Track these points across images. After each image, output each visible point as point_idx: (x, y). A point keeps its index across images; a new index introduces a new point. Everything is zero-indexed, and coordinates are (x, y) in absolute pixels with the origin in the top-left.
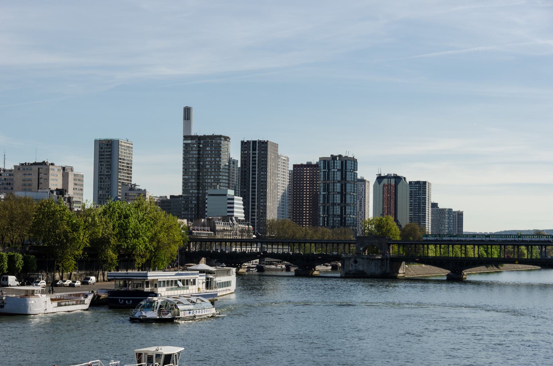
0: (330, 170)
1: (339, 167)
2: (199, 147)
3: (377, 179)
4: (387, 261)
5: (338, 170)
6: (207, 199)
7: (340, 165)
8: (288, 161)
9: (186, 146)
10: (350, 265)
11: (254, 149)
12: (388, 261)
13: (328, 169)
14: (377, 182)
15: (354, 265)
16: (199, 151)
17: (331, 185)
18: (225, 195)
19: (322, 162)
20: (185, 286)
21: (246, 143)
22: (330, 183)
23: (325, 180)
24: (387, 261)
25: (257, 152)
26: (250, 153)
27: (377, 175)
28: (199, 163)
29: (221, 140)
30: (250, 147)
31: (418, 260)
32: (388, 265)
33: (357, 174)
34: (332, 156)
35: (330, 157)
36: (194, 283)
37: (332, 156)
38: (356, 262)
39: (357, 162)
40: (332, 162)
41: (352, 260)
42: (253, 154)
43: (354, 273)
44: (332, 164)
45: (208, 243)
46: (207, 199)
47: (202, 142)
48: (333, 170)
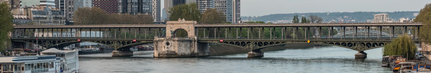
4: (194, 43)
10: (163, 47)
12: (196, 43)
15: (166, 46)
20: (37, 69)
24: (194, 43)
31: (223, 41)
32: (196, 46)
36: (52, 66)
38: (168, 44)
41: (165, 42)
43: (166, 54)
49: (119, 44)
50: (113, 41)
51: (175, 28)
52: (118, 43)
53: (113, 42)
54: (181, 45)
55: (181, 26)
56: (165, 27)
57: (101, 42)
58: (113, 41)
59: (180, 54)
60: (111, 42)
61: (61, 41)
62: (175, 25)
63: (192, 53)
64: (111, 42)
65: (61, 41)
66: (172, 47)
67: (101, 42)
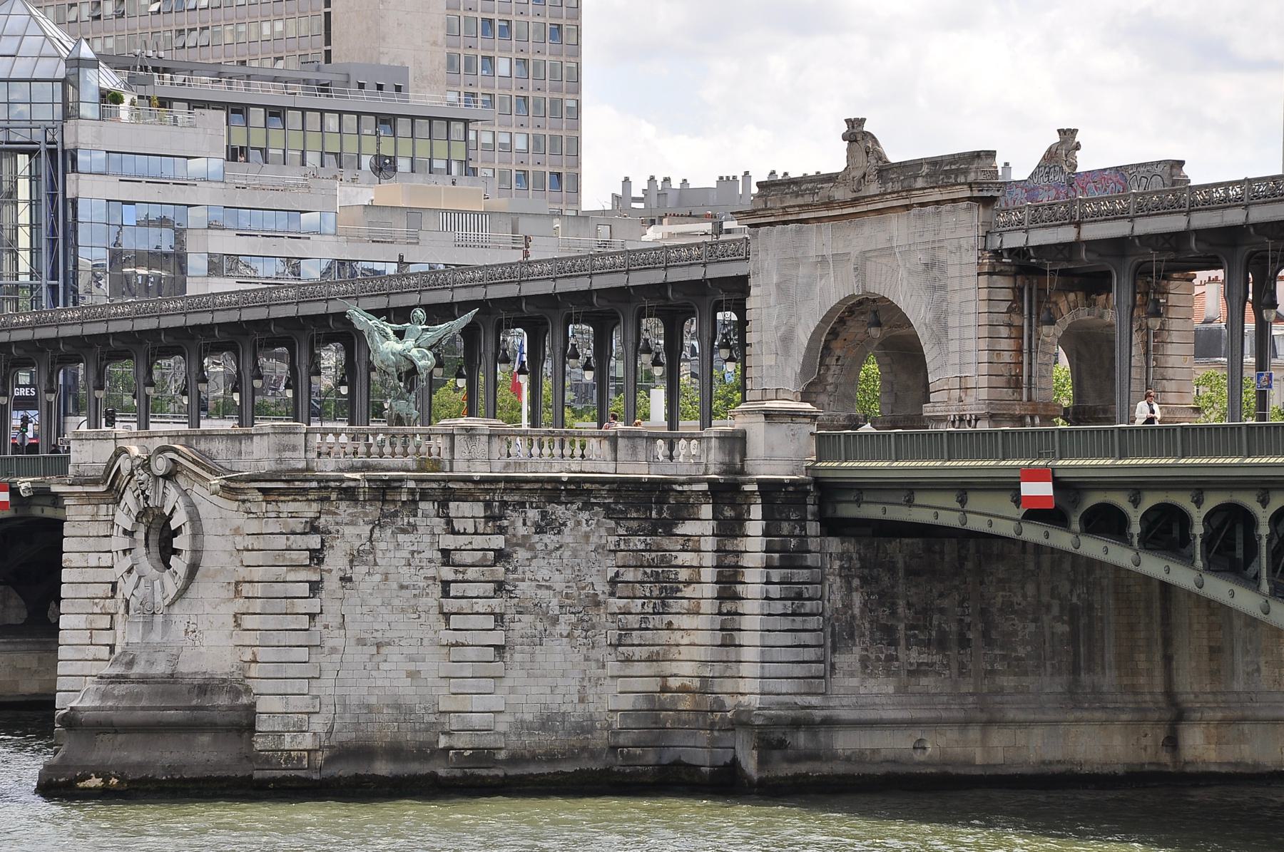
4: (730, 528)
24: (730, 528)
54: (336, 561)
55: (864, 256)
59: (318, 724)
63: (686, 703)
66: (207, 591)
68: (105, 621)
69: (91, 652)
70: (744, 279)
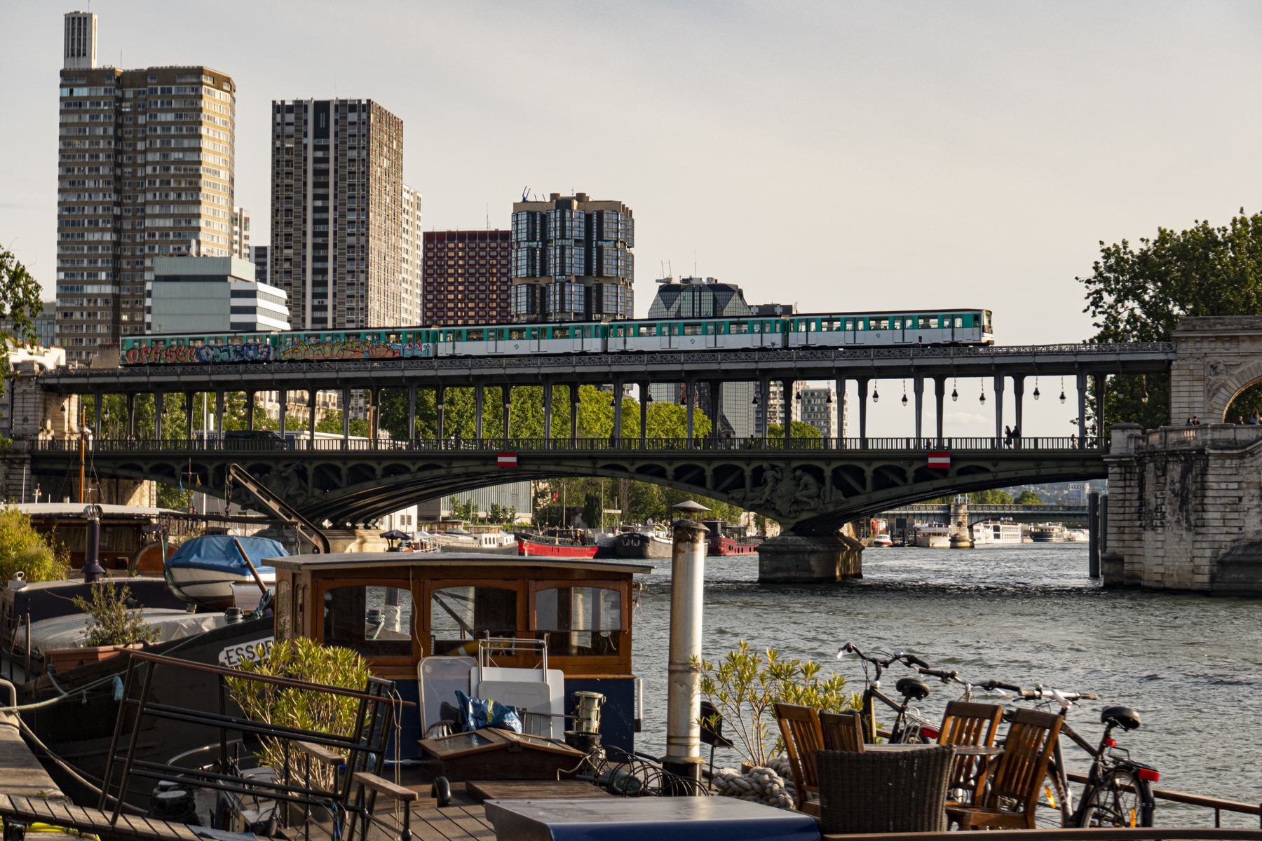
0: (550, 241)
1: (578, 231)
2: (119, 113)
3: (660, 292)
5: (576, 241)
6: (149, 294)
7: (583, 225)
8: (419, 208)
9: (69, 106)
11: (321, 132)
13: (541, 240)
14: (661, 302)
16: (118, 126)
17: (553, 290)
18: (223, 278)
19: (525, 216)
21: (290, 109)
22: (547, 285)
23: (534, 276)
25: (332, 142)
26: (306, 146)
27: (657, 281)
28: (119, 132)
29: (201, 84)
30: (306, 122)
33: (633, 256)
34: (554, 196)
35: (548, 199)
37: (554, 196)
39: (633, 221)
40: (554, 216)
42: (316, 148)
44: (554, 225)
45: (178, 399)
46: (149, 294)
47: (129, 93)
48: (559, 242)
49: (813, 490)
50: (765, 465)
51: (1241, 369)
52: (808, 478)
53: (769, 474)
56: (1163, 361)
57: (670, 470)
58: (765, 465)
60: (748, 471)
61: (379, 470)
62: (1246, 347)
64: (748, 471)
65: (372, 470)
67: (670, 470)
68: (1235, 515)
69: (1225, 530)
70: (1170, 362)
